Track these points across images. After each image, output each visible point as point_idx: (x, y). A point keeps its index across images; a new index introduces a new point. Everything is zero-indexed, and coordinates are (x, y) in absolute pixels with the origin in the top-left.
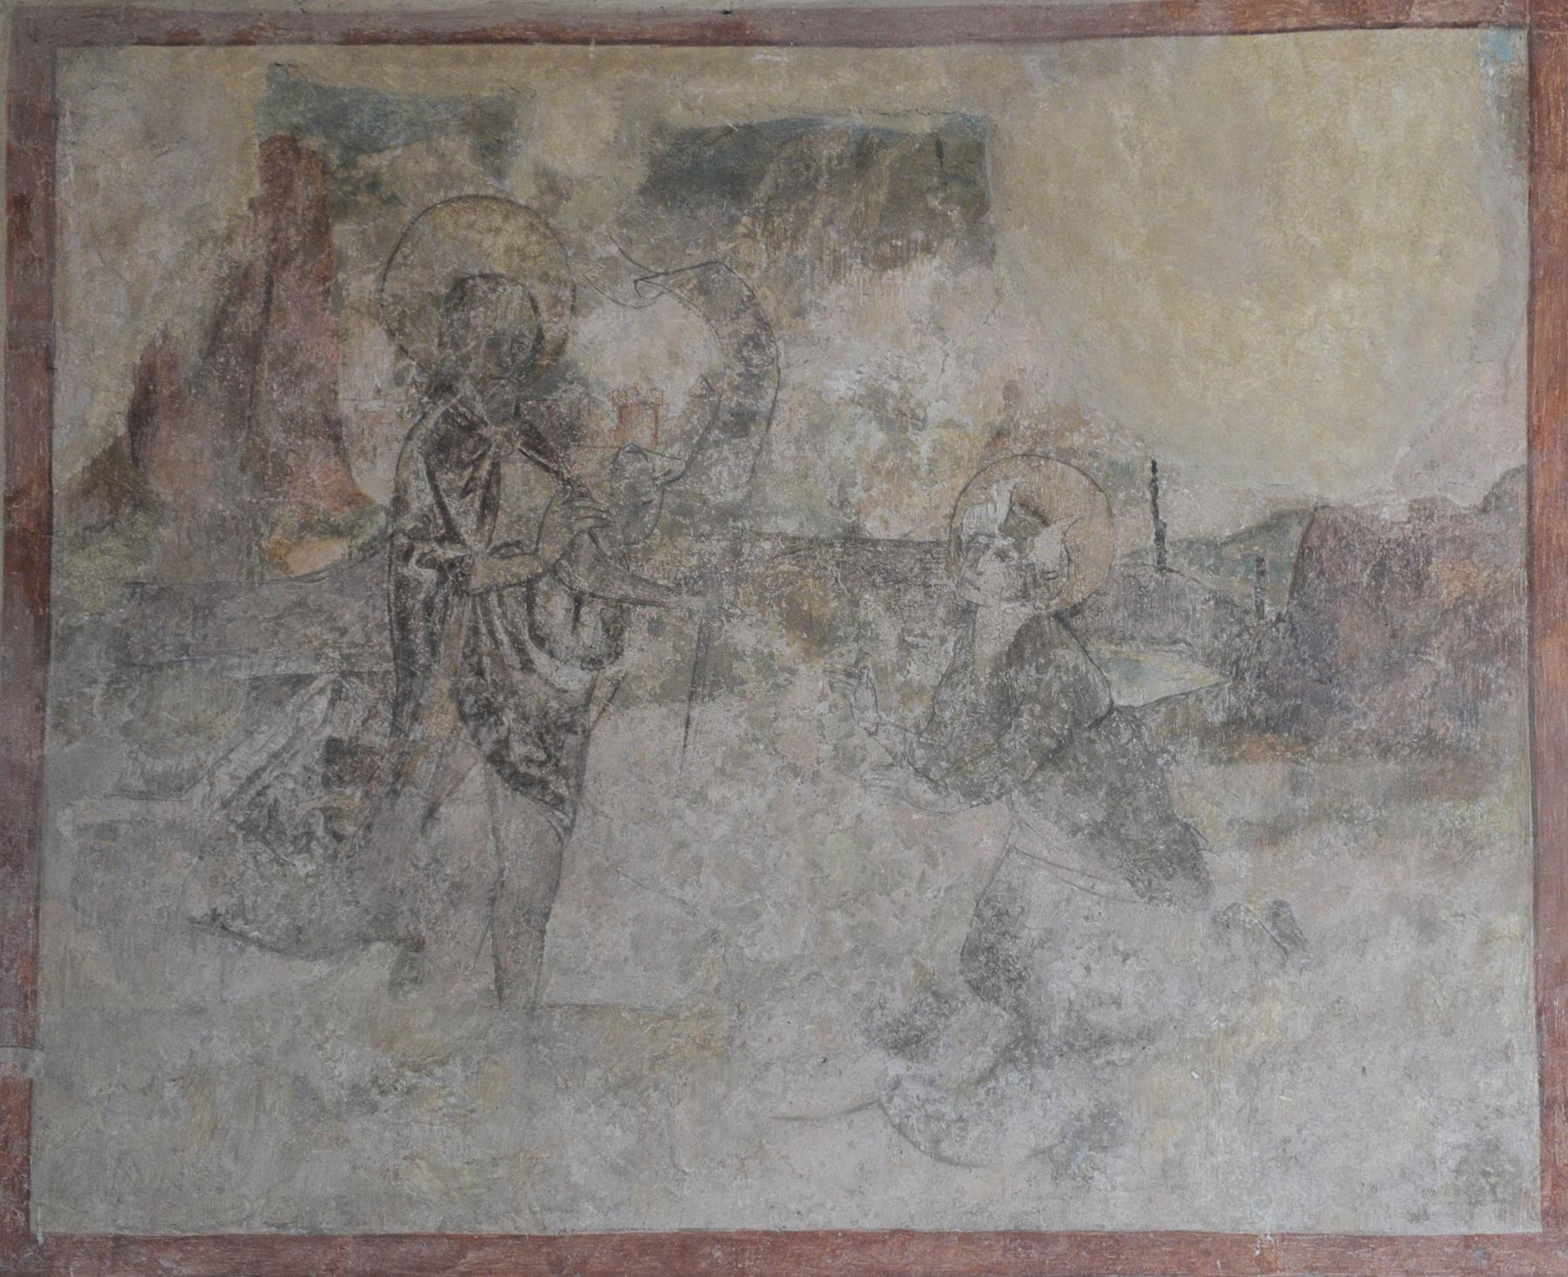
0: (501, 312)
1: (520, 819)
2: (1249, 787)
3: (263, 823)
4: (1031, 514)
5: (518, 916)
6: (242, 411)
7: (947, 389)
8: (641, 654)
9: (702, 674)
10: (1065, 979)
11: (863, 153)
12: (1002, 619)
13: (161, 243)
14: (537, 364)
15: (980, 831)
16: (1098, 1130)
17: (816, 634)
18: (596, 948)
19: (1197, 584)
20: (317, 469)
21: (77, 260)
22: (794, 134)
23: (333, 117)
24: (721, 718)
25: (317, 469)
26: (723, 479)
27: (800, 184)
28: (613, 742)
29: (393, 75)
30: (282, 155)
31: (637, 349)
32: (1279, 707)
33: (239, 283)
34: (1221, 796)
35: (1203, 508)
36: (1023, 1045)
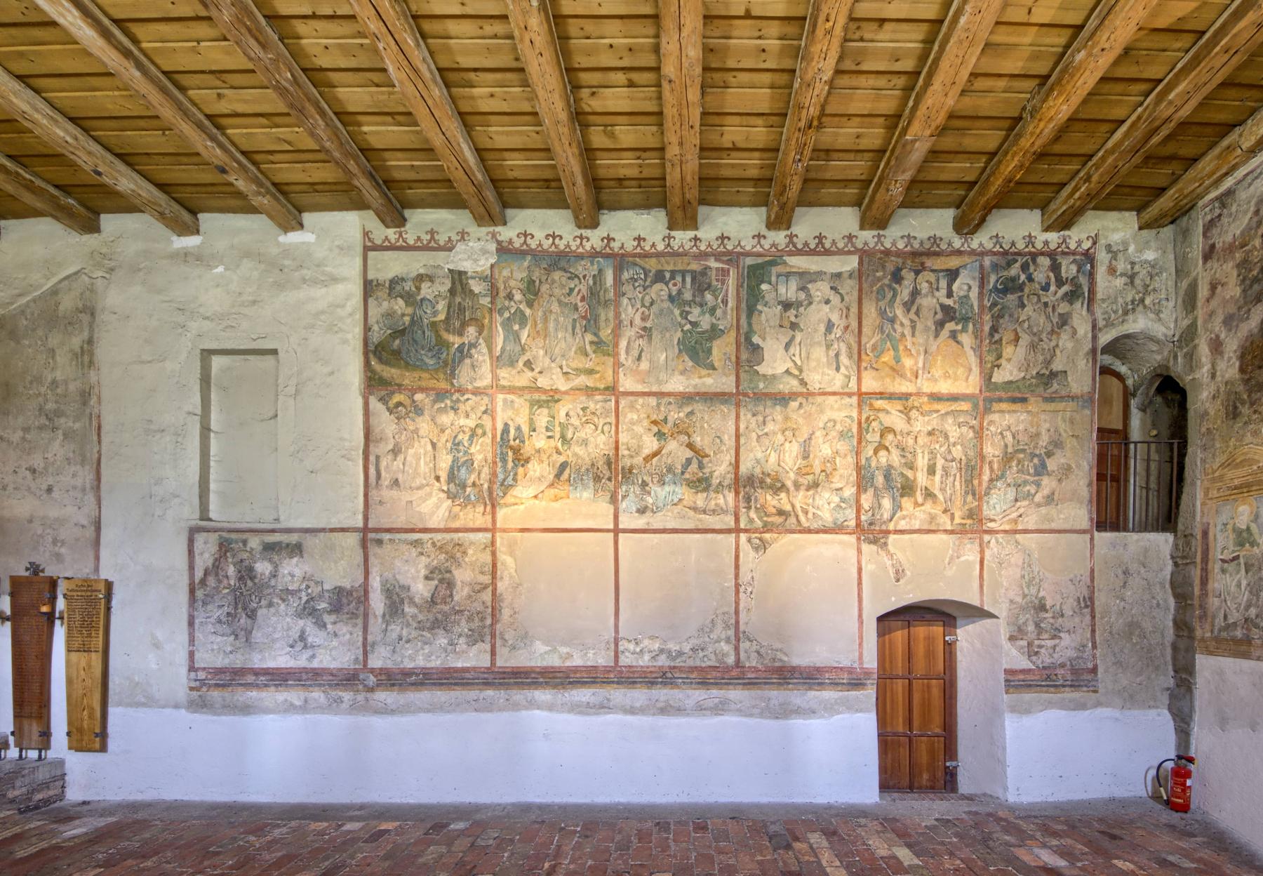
0: (246, 563)
1: (249, 621)
2: (333, 617)
3: (220, 621)
4: (308, 587)
5: (249, 633)
6: (217, 575)
7: (298, 572)
8: (263, 602)
9: (270, 605)
10: (310, 640)
11: (288, 545)
12: (305, 599)
13: (206, 555)
14: (251, 569)
15: (301, 623)
16: (313, 656)
17: (284, 600)
18: (257, 636)
19: (327, 595)
20: (225, 581)
21: (197, 557)
22: (279, 543)
23: (226, 540)
24: (272, 610)
25: (225, 581)
26: (273, 582)
27: (281, 548)
28: (260, 612)
29: (234, 536)
30: (221, 545)
31: (263, 568)
32: (336, 608)
33: (216, 560)
34: (328, 619)
35: (326, 587)
36: (305, 647)
